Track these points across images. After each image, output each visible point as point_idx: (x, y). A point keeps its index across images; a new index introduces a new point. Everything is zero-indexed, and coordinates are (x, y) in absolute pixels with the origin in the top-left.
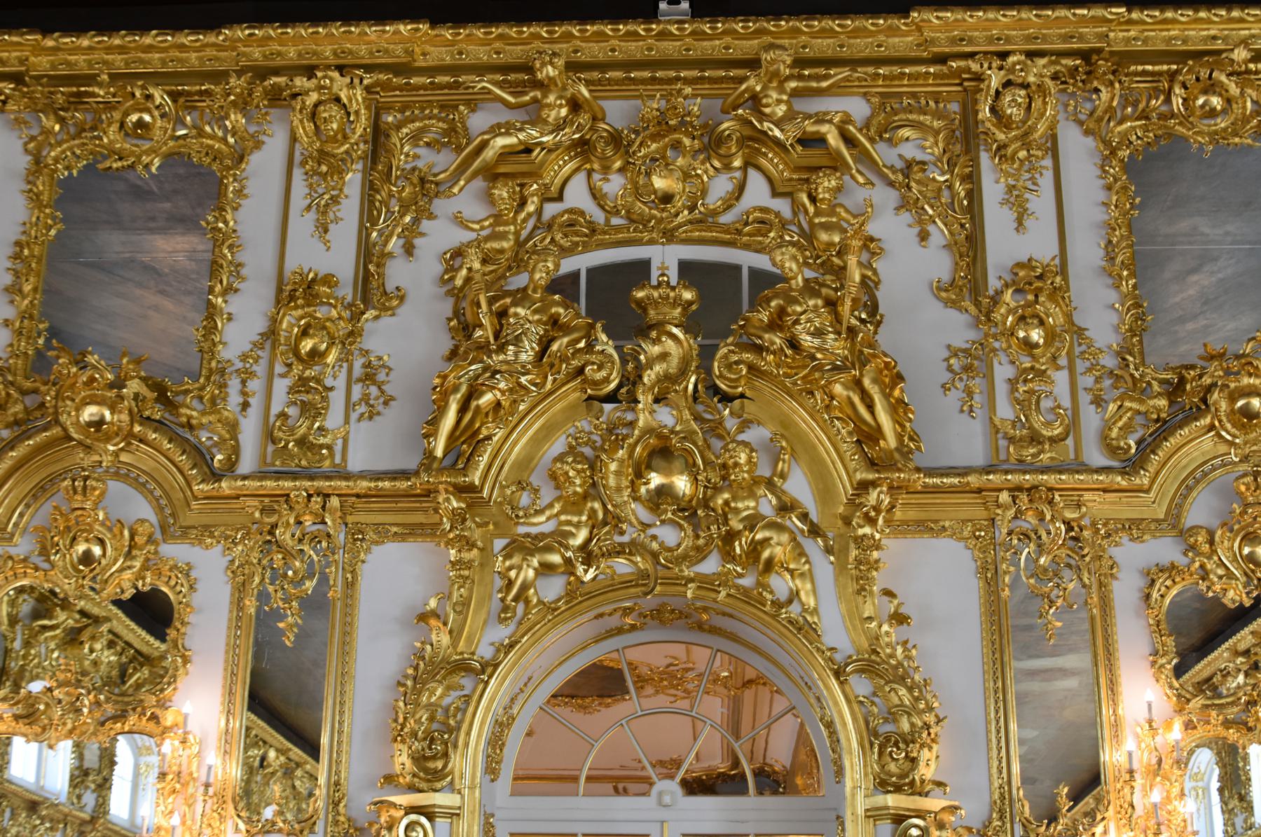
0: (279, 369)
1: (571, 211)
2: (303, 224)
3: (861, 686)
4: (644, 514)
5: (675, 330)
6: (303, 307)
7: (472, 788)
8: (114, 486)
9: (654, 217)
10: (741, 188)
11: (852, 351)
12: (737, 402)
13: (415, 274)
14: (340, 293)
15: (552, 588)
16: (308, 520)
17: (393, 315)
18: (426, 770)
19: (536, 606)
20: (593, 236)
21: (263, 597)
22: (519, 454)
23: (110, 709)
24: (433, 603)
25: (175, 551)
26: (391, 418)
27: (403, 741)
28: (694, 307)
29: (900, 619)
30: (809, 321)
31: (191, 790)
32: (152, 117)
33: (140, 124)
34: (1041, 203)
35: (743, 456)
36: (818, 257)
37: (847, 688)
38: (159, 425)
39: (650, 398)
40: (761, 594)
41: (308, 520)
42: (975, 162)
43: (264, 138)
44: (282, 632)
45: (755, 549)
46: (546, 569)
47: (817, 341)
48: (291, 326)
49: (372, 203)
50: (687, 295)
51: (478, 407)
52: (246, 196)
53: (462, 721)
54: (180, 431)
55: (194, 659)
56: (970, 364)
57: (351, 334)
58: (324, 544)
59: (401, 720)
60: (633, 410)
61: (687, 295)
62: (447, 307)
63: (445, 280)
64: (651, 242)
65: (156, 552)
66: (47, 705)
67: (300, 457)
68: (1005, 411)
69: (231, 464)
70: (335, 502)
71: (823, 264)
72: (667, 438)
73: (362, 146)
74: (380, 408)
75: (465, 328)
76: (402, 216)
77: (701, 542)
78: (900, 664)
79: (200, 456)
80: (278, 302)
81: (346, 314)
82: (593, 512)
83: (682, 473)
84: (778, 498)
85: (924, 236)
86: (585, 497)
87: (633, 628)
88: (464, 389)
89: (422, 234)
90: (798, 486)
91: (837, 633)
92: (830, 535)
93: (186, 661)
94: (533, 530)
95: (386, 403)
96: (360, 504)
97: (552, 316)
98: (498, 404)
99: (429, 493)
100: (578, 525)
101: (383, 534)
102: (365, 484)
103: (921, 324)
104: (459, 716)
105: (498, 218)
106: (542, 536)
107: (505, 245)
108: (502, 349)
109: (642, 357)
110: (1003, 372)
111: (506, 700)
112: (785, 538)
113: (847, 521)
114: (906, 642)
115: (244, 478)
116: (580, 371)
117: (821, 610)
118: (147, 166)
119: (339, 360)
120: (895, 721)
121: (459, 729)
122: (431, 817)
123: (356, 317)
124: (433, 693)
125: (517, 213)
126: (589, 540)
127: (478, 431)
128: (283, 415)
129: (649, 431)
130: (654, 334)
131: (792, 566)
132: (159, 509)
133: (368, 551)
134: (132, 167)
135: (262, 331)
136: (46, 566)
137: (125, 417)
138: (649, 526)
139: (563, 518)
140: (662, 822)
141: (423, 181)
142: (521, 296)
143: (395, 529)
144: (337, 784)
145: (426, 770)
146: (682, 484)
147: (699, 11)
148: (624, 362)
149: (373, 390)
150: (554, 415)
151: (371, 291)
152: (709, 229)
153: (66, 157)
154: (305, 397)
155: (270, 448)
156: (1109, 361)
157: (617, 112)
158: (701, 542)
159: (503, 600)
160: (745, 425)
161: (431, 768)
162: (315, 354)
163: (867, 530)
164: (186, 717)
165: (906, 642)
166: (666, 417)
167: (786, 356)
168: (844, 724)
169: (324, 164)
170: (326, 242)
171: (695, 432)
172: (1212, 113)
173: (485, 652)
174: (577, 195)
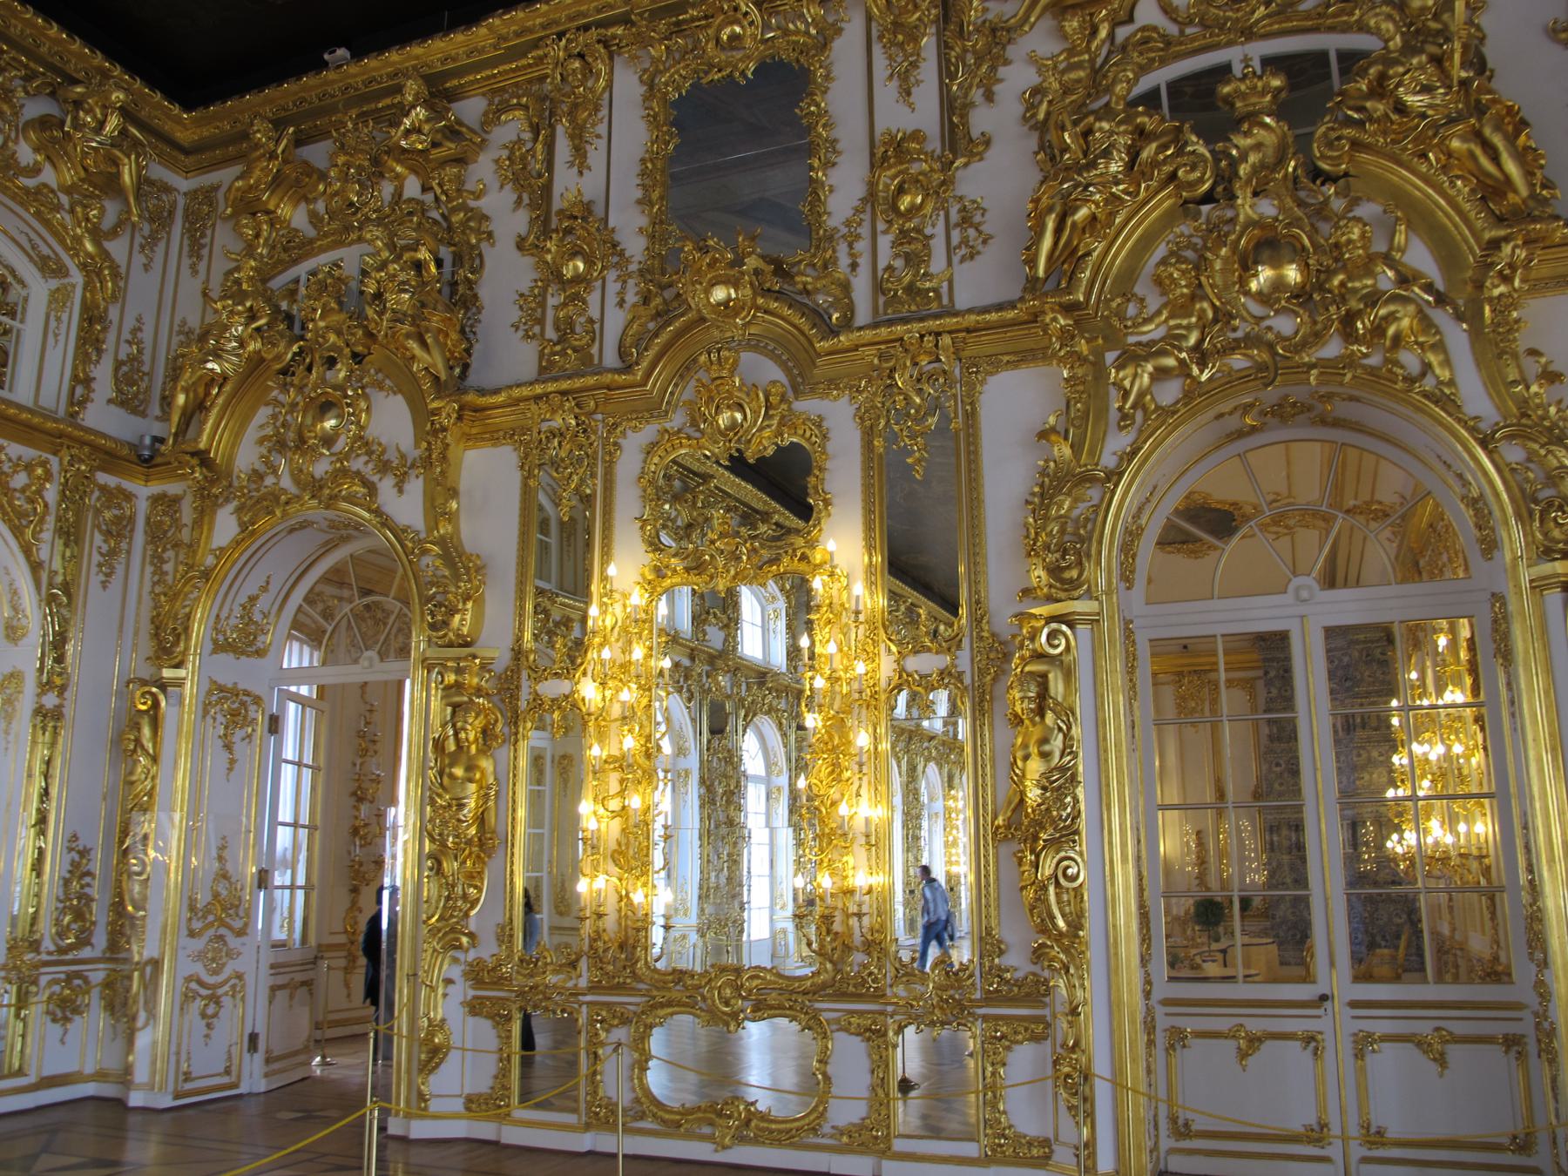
0: (881, 226)
1: (1143, 29)
2: (887, 92)
3: (1513, 453)
4: (1256, 309)
5: (1268, 120)
6: (895, 165)
7: (1108, 593)
8: (745, 356)
9: (1229, 18)
11: (1467, 103)
12: (1342, 182)
13: (998, 118)
14: (929, 148)
15: (1169, 393)
16: (924, 361)
17: (981, 159)
18: (1063, 581)
19: (1154, 411)
20: (1170, 49)
21: (893, 438)
22: (1121, 266)
23: (766, 554)
24: (1052, 420)
25: (808, 406)
26: (991, 256)
27: (1037, 555)
28: (1283, 95)
29: (1551, 377)
30: (1413, 79)
31: (844, 620)
32: (742, 27)
33: (734, 37)
35: (1356, 230)
36: (1411, 24)
37: (1496, 456)
38: (779, 295)
39: (1249, 191)
40: (1390, 371)
41: (924, 361)
43: (843, 25)
44: (911, 467)
46: (1161, 374)
47: (1425, 98)
48: (887, 186)
49: (948, 61)
50: (1276, 83)
51: (1074, 224)
52: (833, 79)
53: (1093, 530)
54: (798, 298)
55: (834, 501)
57: (943, 183)
58: (941, 380)
59: (1033, 535)
60: (1232, 207)
61: (1276, 83)
62: (1033, 143)
63: (1028, 118)
64: (1230, 44)
65: (790, 409)
66: (712, 556)
67: (908, 299)
69: (847, 324)
70: (946, 340)
71: (1418, 31)
72: (1272, 227)
73: (933, 11)
74: (980, 248)
75: (1050, 153)
76: (978, 67)
77: (1319, 327)
78: (1555, 425)
79: (818, 317)
80: (872, 166)
81: (937, 166)
82: (1203, 311)
83: (1292, 262)
84: (1398, 272)
86: (1193, 298)
87: (1253, 429)
88: (1058, 208)
89: (1000, 81)
91: (1476, 399)
92: (1461, 302)
93: (827, 503)
94: (1144, 339)
95: (985, 242)
96: (971, 338)
97: (1138, 126)
98: (1093, 218)
99: (1035, 317)
100: (1189, 328)
101: (995, 364)
102: (973, 317)
104: (1089, 526)
105: (1071, 52)
106: (1153, 343)
107: (1082, 74)
108: (1093, 165)
109: (1234, 152)
111: (1134, 509)
112: (1411, 308)
113: (1479, 286)
114: (1560, 402)
115: (860, 329)
116: (1173, 176)
117: (1458, 380)
118: (743, 73)
119: (935, 209)
120: (1555, 485)
121: (1090, 539)
122: (1071, 625)
123: (947, 166)
124: (1060, 507)
125: (1089, 42)
126: (1201, 341)
127: (1076, 249)
128: (889, 268)
129: (1250, 223)
130: (1245, 127)
131: (1421, 339)
132: (783, 365)
133: (983, 382)
134: (730, 75)
135: (861, 195)
136: (698, 435)
137: (748, 291)
138: (1262, 318)
139: (1172, 323)
140: (1302, 617)
141: (994, 31)
142: (1107, 112)
143: (1006, 358)
144: (978, 602)
145: (1063, 581)
146: (1292, 274)
148: (1217, 160)
149: (971, 232)
150: (1150, 225)
151: (959, 140)
152: (1289, 20)
153: (675, 82)
154: (907, 248)
155: (881, 300)
158: (1319, 327)
159: (1120, 409)
160: (1355, 202)
162: (914, 210)
163: (1502, 289)
164: (831, 554)
165: (1560, 402)
166: (1267, 208)
167: (1392, 122)
168: (1497, 495)
170: (910, 105)
171: (1300, 219)
173: (1108, 460)
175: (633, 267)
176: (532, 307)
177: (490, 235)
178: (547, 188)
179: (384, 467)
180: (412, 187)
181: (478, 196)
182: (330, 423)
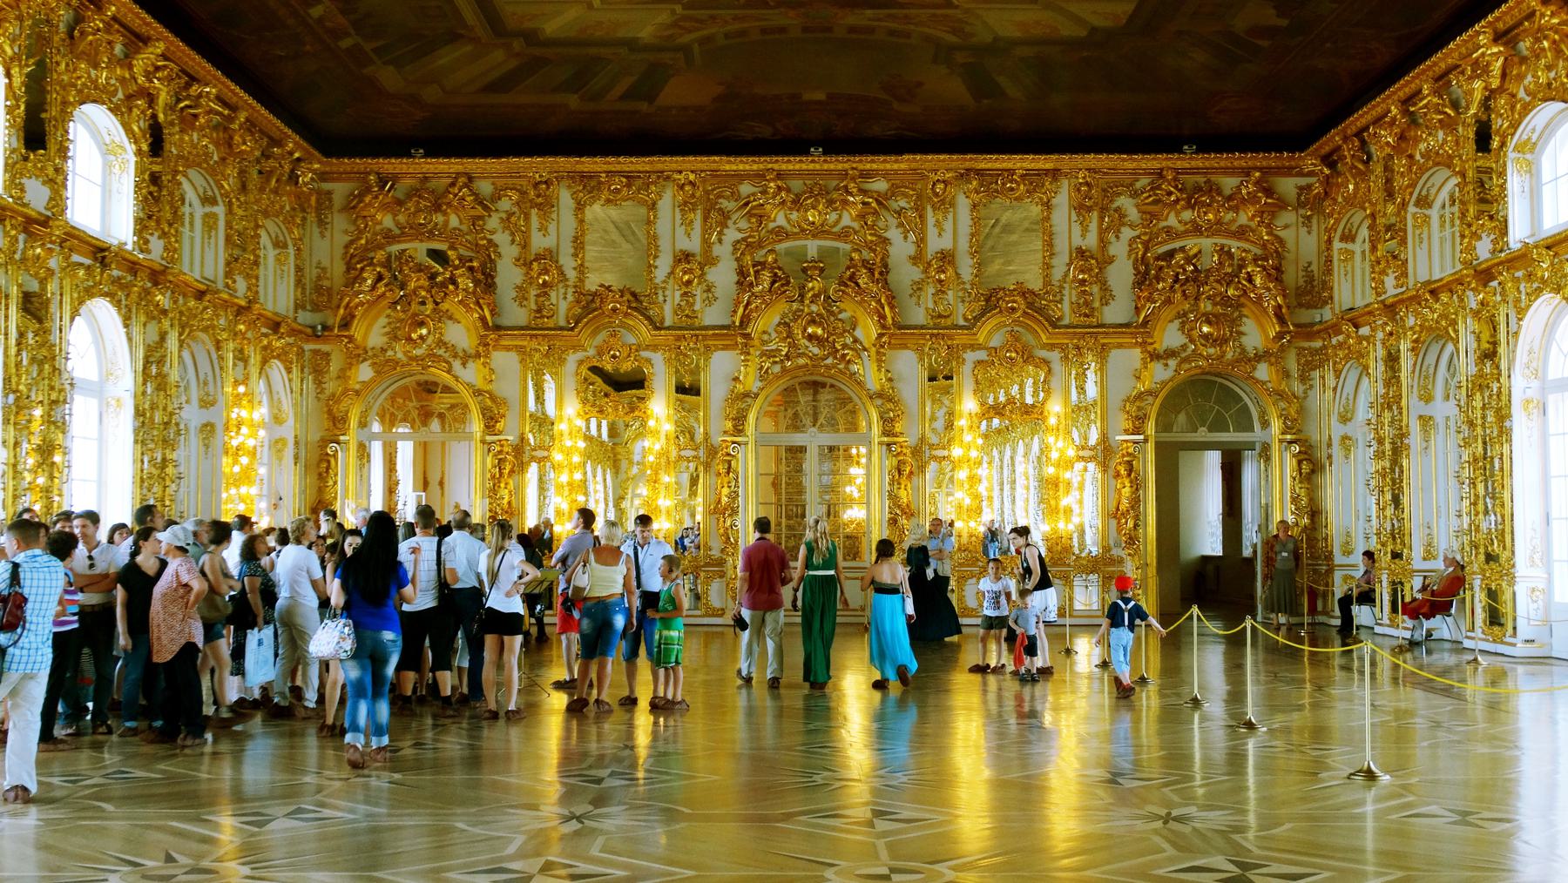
2: (680, 231)
13: (723, 251)
15: (777, 369)
25: (645, 354)
34: (948, 226)
42: (924, 209)
45: (844, 356)
56: (918, 287)
62: (735, 265)
68: (931, 305)
75: (742, 273)
90: (858, 333)
103: (905, 273)
110: (931, 290)
115: (668, 328)
146: (820, 331)
147: (825, 153)
156: (968, 286)
157: (797, 185)
161: (739, 430)
162: (689, 282)
166: (814, 308)
169: (686, 206)
172: (1012, 189)
174: (781, 220)
176: (521, 295)
177: (500, 255)
179: (455, 356)
181: (492, 233)
182: (424, 331)
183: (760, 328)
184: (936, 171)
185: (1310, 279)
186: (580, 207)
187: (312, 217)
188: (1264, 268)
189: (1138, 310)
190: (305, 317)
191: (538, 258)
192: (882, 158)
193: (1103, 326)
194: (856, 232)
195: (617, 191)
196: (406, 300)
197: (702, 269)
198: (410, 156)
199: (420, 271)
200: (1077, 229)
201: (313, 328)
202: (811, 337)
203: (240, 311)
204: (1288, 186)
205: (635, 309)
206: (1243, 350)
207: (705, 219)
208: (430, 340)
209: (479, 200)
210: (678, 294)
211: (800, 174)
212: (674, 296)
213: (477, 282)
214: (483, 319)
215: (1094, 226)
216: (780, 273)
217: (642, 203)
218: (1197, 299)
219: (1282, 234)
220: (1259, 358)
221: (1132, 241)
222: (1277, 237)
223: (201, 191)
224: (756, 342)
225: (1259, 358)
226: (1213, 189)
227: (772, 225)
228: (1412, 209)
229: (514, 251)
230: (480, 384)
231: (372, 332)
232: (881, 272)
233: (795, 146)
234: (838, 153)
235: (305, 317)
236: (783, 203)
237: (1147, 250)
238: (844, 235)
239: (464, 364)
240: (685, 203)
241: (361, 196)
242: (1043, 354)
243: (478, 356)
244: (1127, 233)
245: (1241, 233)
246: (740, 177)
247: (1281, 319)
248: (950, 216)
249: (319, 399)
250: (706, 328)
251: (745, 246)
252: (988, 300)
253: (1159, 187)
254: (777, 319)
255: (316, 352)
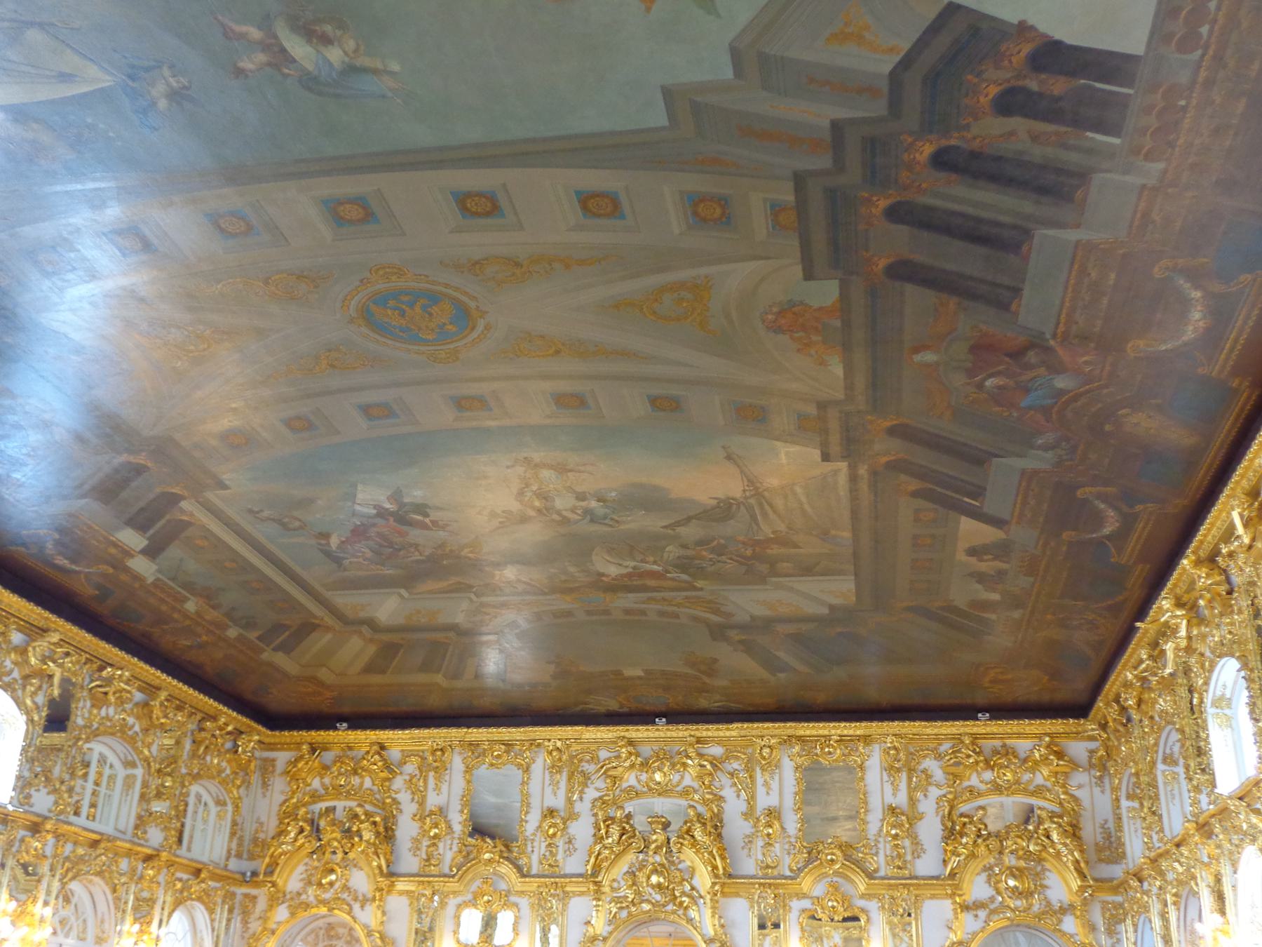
2: (548, 790)
10: (682, 777)
13: (583, 808)
15: (624, 914)
34: (775, 785)
42: (753, 770)
56: (749, 840)
68: (760, 857)
85: (738, 796)
90: (695, 882)
103: (737, 827)
110: (760, 843)
115: (533, 876)
147: (668, 723)
156: (793, 840)
162: (554, 835)
166: (658, 858)
169: (555, 768)
172: (830, 753)
175: (456, 835)
177: (401, 811)
178: (424, 798)
179: (356, 899)
180: (368, 783)
182: (333, 877)
183: (611, 877)
184: (762, 737)
185: (1108, 836)
186: (468, 770)
187: (255, 779)
188: (1060, 825)
189: (945, 862)
190: (234, 864)
191: (432, 813)
192: (715, 727)
193: (916, 878)
194: (695, 791)
195: (499, 757)
196: (320, 850)
197: (564, 823)
198: (336, 729)
199: (334, 825)
200: (888, 788)
201: (244, 874)
202: (653, 887)
203: (148, 859)
204: (1079, 749)
205: (507, 859)
206: (1049, 903)
207: (569, 779)
208: (337, 885)
209: (388, 767)
210: (544, 845)
211: (648, 741)
212: (540, 847)
213: (378, 834)
214: (380, 867)
215: (903, 785)
216: (627, 827)
217: (519, 766)
218: (1001, 853)
219: (1077, 793)
220: (1065, 910)
221: (939, 799)
222: (1072, 796)
223: (122, 756)
224: (607, 889)
225: (1065, 910)
226: (1008, 752)
227: (625, 785)
228: (1160, 766)
229: (413, 808)
230: (373, 924)
231: (292, 880)
232: (716, 826)
233: (644, 717)
234: (678, 723)
235: (234, 864)
236: (632, 766)
237: (952, 808)
238: (686, 793)
239: (362, 907)
240: (553, 767)
241: (297, 760)
242: (862, 903)
243: (374, 899)
244: (934, 792)
245: (1038, 791)
246: (600, 743)
247: (1083, 876)
248: (777, 777)
249: (243, 938)
250: (565, 876)
251: (601, 802)
252: (809, 853)
253: (959, 751)
254: (625, 869)
255: (246, 895)
